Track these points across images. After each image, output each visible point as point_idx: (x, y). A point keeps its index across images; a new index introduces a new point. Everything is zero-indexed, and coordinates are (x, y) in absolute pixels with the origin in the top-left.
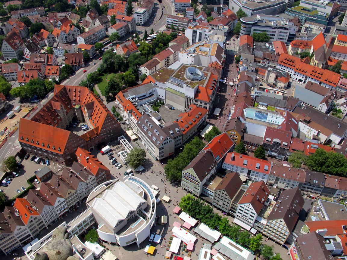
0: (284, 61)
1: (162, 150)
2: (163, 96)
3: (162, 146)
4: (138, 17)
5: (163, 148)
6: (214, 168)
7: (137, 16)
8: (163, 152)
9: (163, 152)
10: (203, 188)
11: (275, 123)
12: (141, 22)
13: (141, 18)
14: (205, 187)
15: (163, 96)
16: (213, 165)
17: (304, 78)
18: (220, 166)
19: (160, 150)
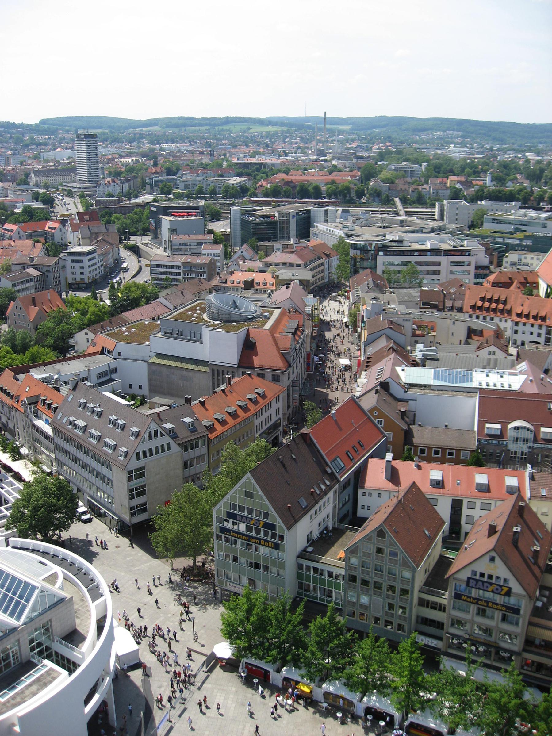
0: (479, 303)
1: (137, 483)
2: (141, 387)
3: (134, 464)
4: (74, 264)
5: (141, 473)
6: (331, 494)
7: (72, 261)
8: (142, 475)
9: (141, 492)
10: (301, 567)
11: (499, 387)
12: (82, 276)
13: (82, 268)
14: (305, 563)
15: (141, 387)
16: (325, 484)
17: (543, 336)
18: (349, 506)
19: (130, 479)
